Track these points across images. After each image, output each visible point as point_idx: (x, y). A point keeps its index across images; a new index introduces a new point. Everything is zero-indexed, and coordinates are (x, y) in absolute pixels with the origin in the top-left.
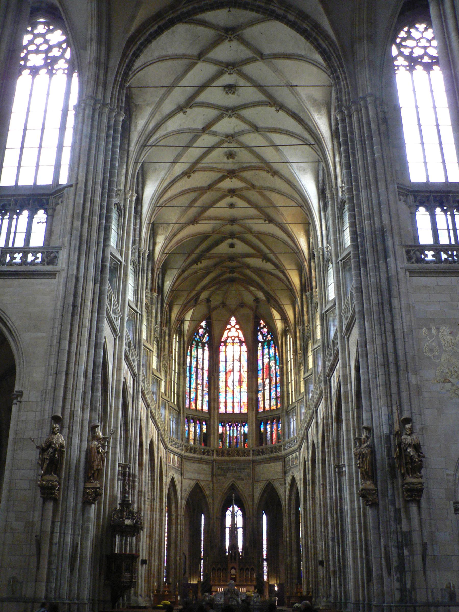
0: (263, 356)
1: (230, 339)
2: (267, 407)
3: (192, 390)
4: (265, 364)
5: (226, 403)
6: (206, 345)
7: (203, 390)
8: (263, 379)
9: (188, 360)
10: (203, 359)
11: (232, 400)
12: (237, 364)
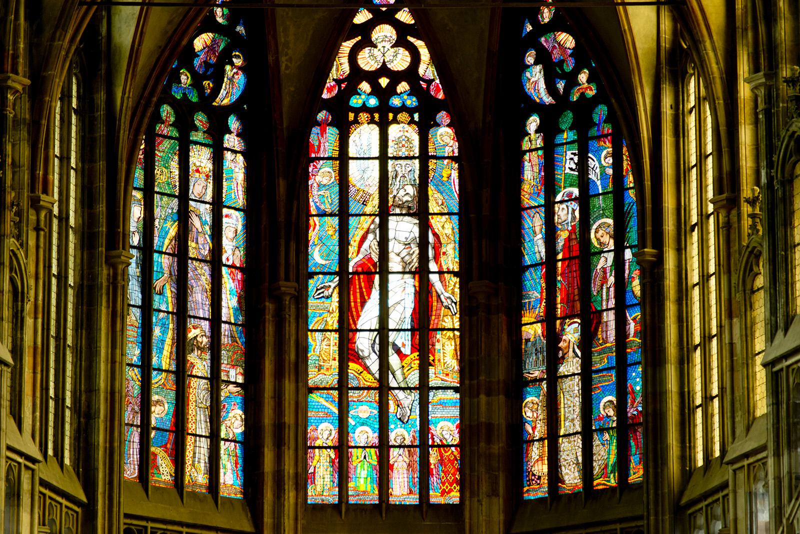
0: (550, 185)
1: (365, 86)
2: (571, 477)
3: (157, 378)
4: (563, 236)
5: (342, 448)
6: (234, 123)
7: (215, 380)
8: (548, 319)
9: (137, 212)
10: (217, 204)
11: (374, 438)
12: (403, 229)
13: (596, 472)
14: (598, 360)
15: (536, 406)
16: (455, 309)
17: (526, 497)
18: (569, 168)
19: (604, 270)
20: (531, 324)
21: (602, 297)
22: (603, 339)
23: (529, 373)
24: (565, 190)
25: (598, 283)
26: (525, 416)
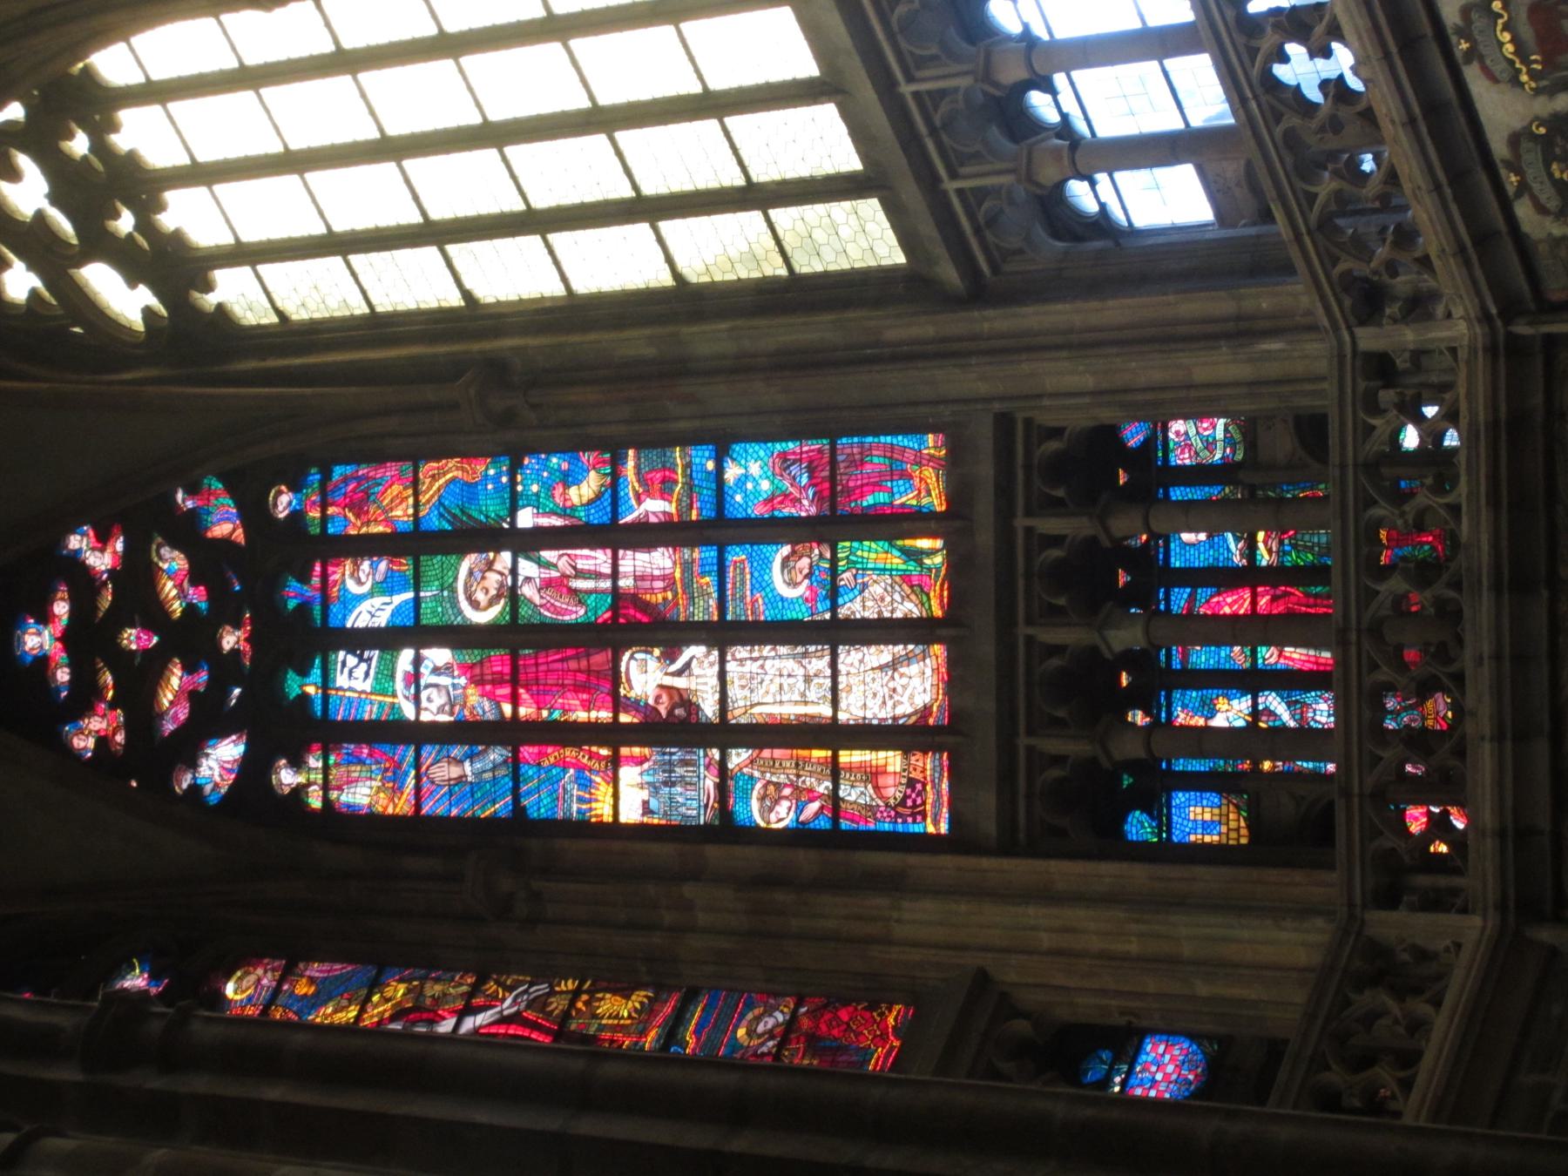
15: (771, 788)
16: (542, 988)
17: (944, 828)
20: (616, 796)
21: (589, 592)
23: (706, 806)
24: (399, 694)
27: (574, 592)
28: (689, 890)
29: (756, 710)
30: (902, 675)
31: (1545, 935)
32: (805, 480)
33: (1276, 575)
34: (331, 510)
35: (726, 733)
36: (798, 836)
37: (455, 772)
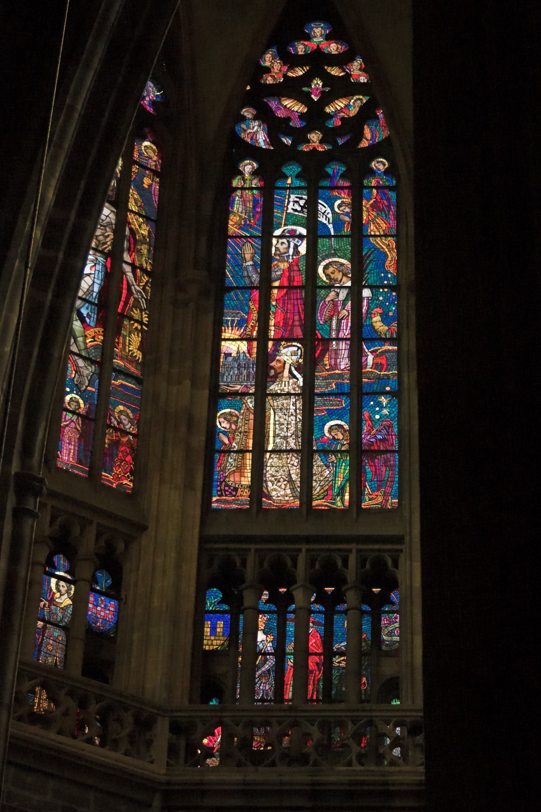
13: (316, 492)
14: (323, 384)
15: (235, 419)
16: (144, 305)
17: (214, 505)
18: (292, 209)
19: (334, 303)
21: (330, 326)
22: (330, 365)
23: (228, 386)
24: (286, 228)
25: (327, 313)
26: (219, 426)
27: (331, 319)
28: (188, 383)
29: (272, 412)
30: (286, 485)
31: (157, 802)
32: (379, 437)
33: (327, 666)
34: (375, 191)
35: (262, 396)
36: (212, 432)
37: (248, 256)
